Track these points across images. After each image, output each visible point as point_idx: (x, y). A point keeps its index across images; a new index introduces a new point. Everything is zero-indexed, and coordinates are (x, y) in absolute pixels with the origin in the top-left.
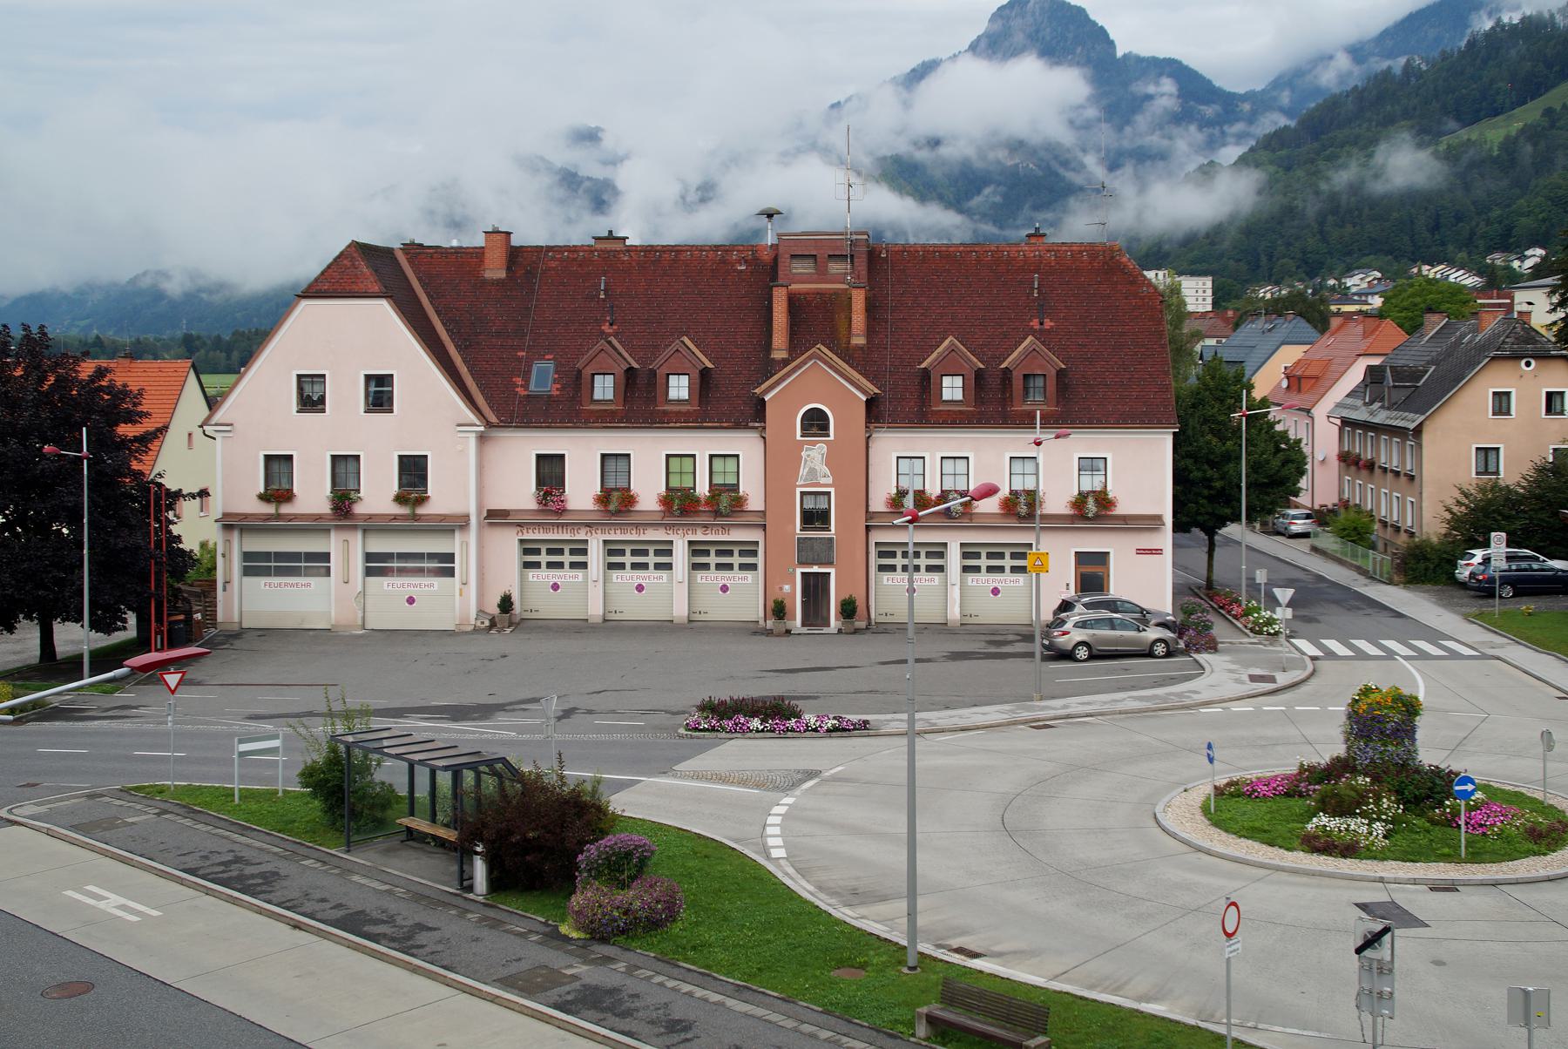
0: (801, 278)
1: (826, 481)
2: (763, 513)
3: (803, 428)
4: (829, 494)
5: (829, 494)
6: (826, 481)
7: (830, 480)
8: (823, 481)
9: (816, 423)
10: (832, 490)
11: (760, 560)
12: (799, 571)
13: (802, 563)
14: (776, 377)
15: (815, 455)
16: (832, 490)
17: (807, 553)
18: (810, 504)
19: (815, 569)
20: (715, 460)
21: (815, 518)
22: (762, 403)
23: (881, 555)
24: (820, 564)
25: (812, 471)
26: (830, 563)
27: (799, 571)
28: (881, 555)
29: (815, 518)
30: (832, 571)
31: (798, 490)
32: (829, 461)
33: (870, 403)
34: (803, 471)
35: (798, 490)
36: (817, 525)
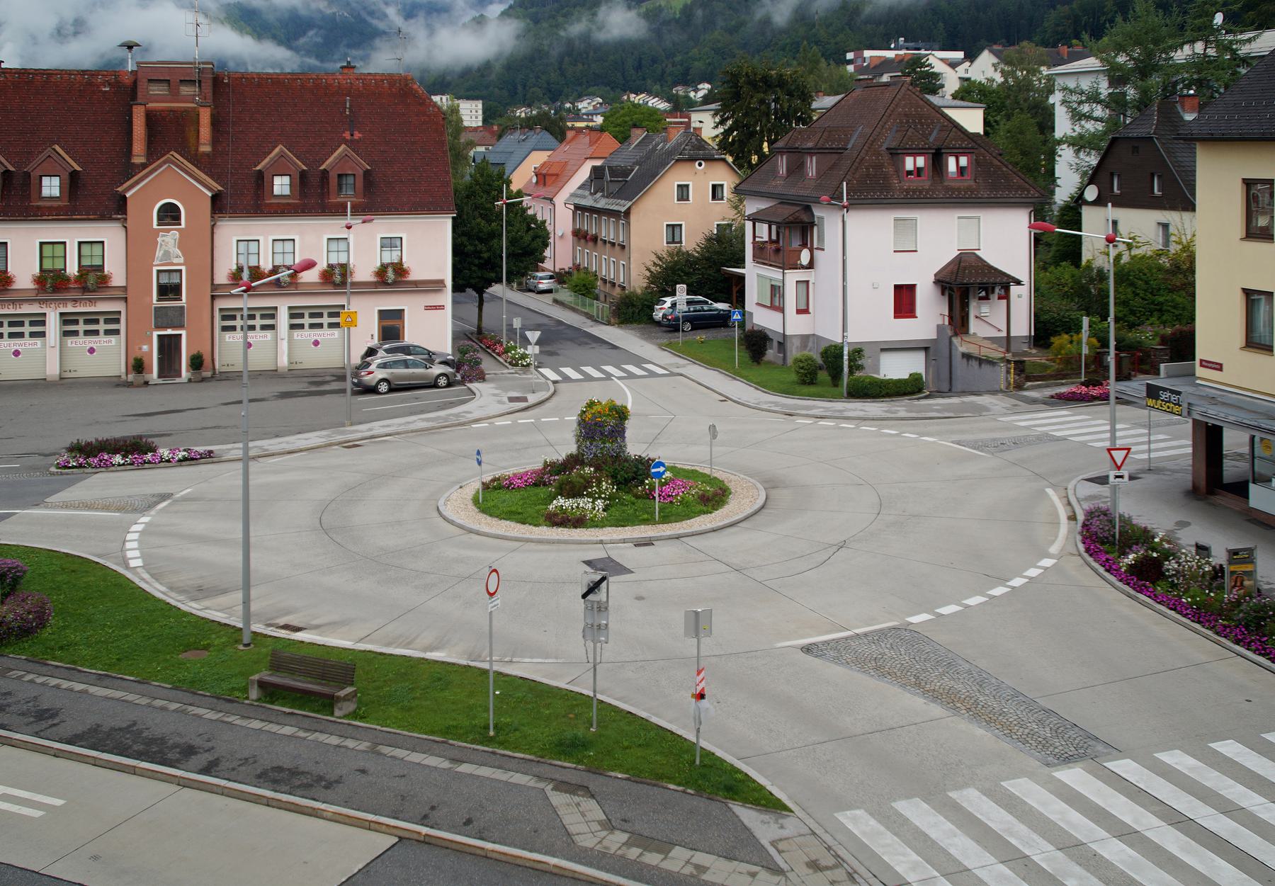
0: (157, 98)
1: (178, 261)
2: (125, 288)
3: (159, 219)
4: (180, 271)
5: (180, 271)
6: (178, 261)
7: (181, 260)
8: (175, 261)
9: (170, 214)
10: (183, 268)
11: (122, 326)
12: (156, 334)
13: (158, 327)
14: (136, 178)
15: (169, 242)
16: (183, 268)
17: (163, 319)
18: (165, 280)
19: (169, 332)
20: (83, 246)
21: (169, 291)
22: (124, 199)
23: (224, 318)
24: (174, 327)
25: (167, 254)
26: (181, 327)
27: (156, 334)
28: (224, 318)
29: (169, 291)
30: (183, 333)
31: (155, 269)
32: (182, 245)
33: (216, 199)
34: (159, 253)
35: (155, 269)
36: (171, 296)
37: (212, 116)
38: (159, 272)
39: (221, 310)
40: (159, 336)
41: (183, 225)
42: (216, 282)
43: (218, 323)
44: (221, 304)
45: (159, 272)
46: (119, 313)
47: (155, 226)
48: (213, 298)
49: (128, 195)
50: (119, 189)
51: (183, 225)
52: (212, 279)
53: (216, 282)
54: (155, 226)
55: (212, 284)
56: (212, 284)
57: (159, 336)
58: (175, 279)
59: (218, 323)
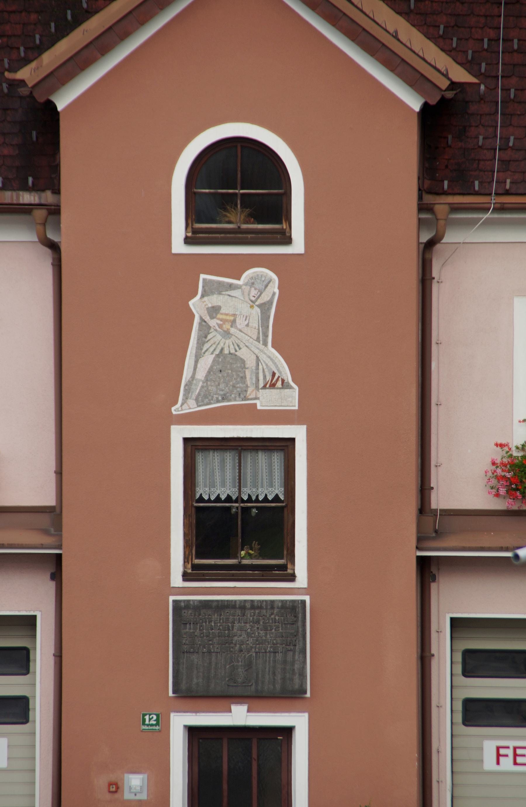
0: (289, 566)
1: (277, 405)
2: (51, 516)
3: (195, 212)
4: (287, 445)
5: (287, 445)
6: (277, 405)
7: (290, 399)
8: (267, 400)
9: (240, 191)
10: (299, 433)
11: (39, 686)
12: (179, 723)
13: (189, 695)
14: (94, 25)
15: (236, 332)
16: (299, 433)
18: (218, 482)
19: (239, 716)
21: (237, 532)
22: (47, 119)
23: (474, 664)
24: (256, 698)
25: (228, 366)
26: (289, 695)
27: (179, 723)
28: (474, 664)
29: (237, 532)
30: (299, 721)
31: (178, 434)
32: (288, 330)
33: (438, 122)
34: (196, 367)
35: (178, 434)
36: (246, 557)
37: (510, 557)
38: (192, 445)
39: (457, 624)
40: (193, 732)
41: (298, 245)
42: (440, 500)
43: (448, 686)
44: (460, 599)
45: (192, 445)
46: (29, 622)
47: (178, 246)
48: (426, 569)
49: (61, 105)
50: (27, 74)
51: (298, 245)
52: (424, 489)
53: (440, 500)
54: (178, 246)
55: (423, 507)
56: (423, 507)
57: (193, 732)
58: (264, 485)
59: (448, 686)
